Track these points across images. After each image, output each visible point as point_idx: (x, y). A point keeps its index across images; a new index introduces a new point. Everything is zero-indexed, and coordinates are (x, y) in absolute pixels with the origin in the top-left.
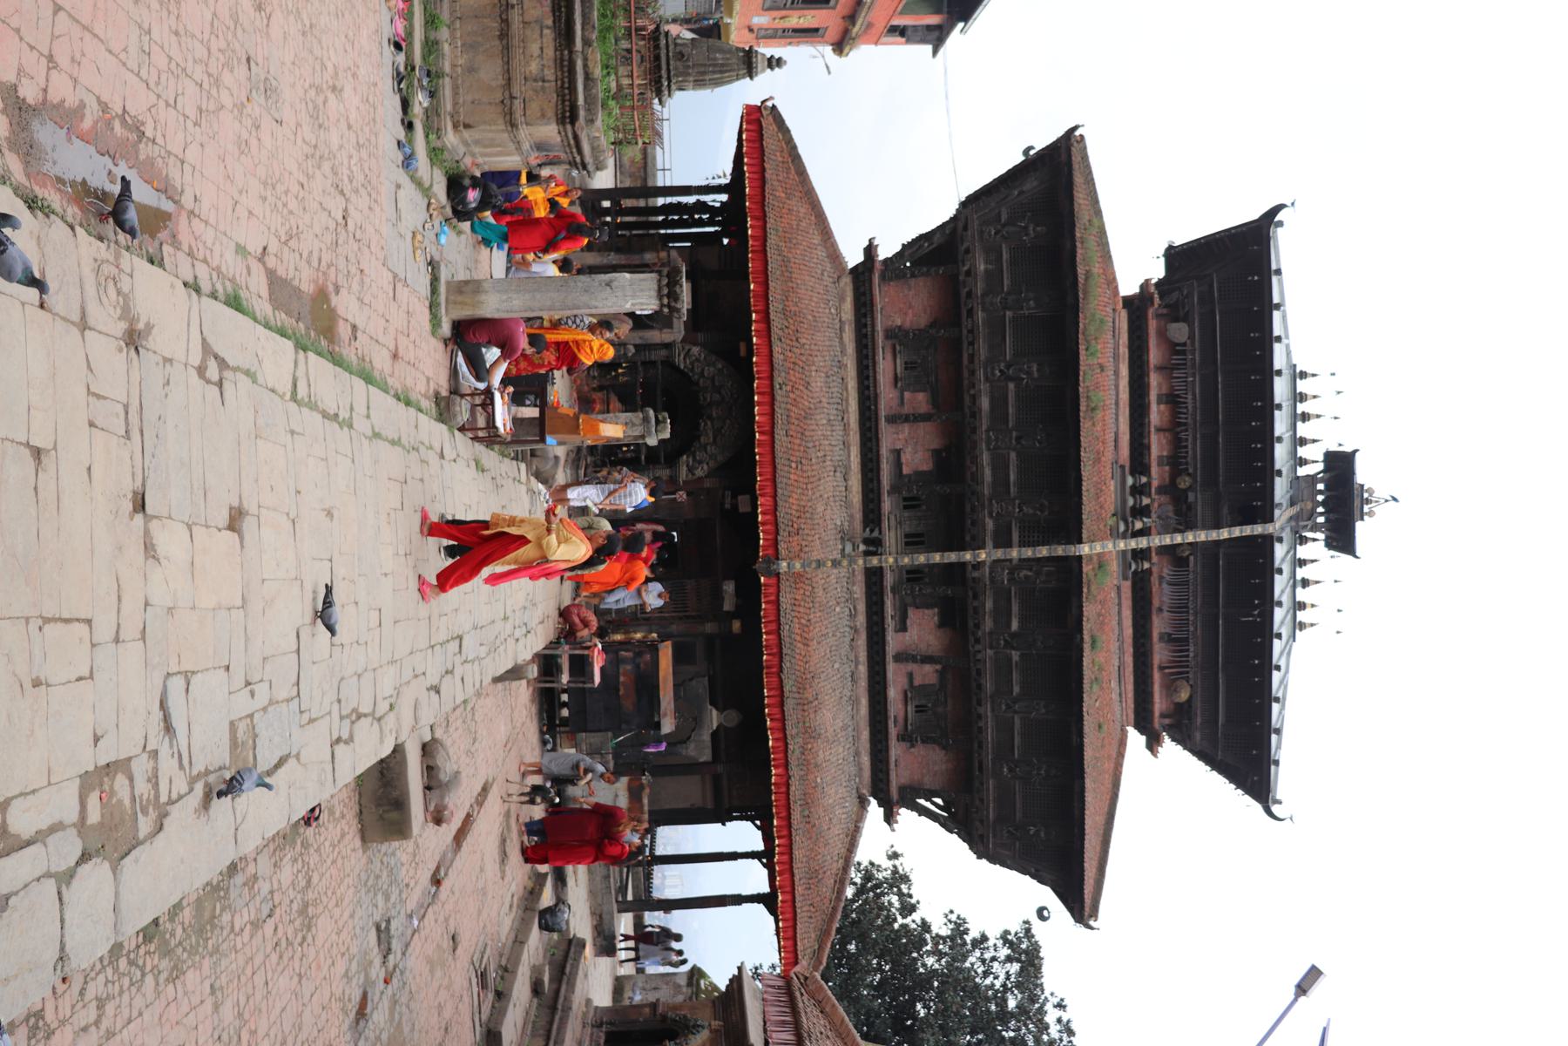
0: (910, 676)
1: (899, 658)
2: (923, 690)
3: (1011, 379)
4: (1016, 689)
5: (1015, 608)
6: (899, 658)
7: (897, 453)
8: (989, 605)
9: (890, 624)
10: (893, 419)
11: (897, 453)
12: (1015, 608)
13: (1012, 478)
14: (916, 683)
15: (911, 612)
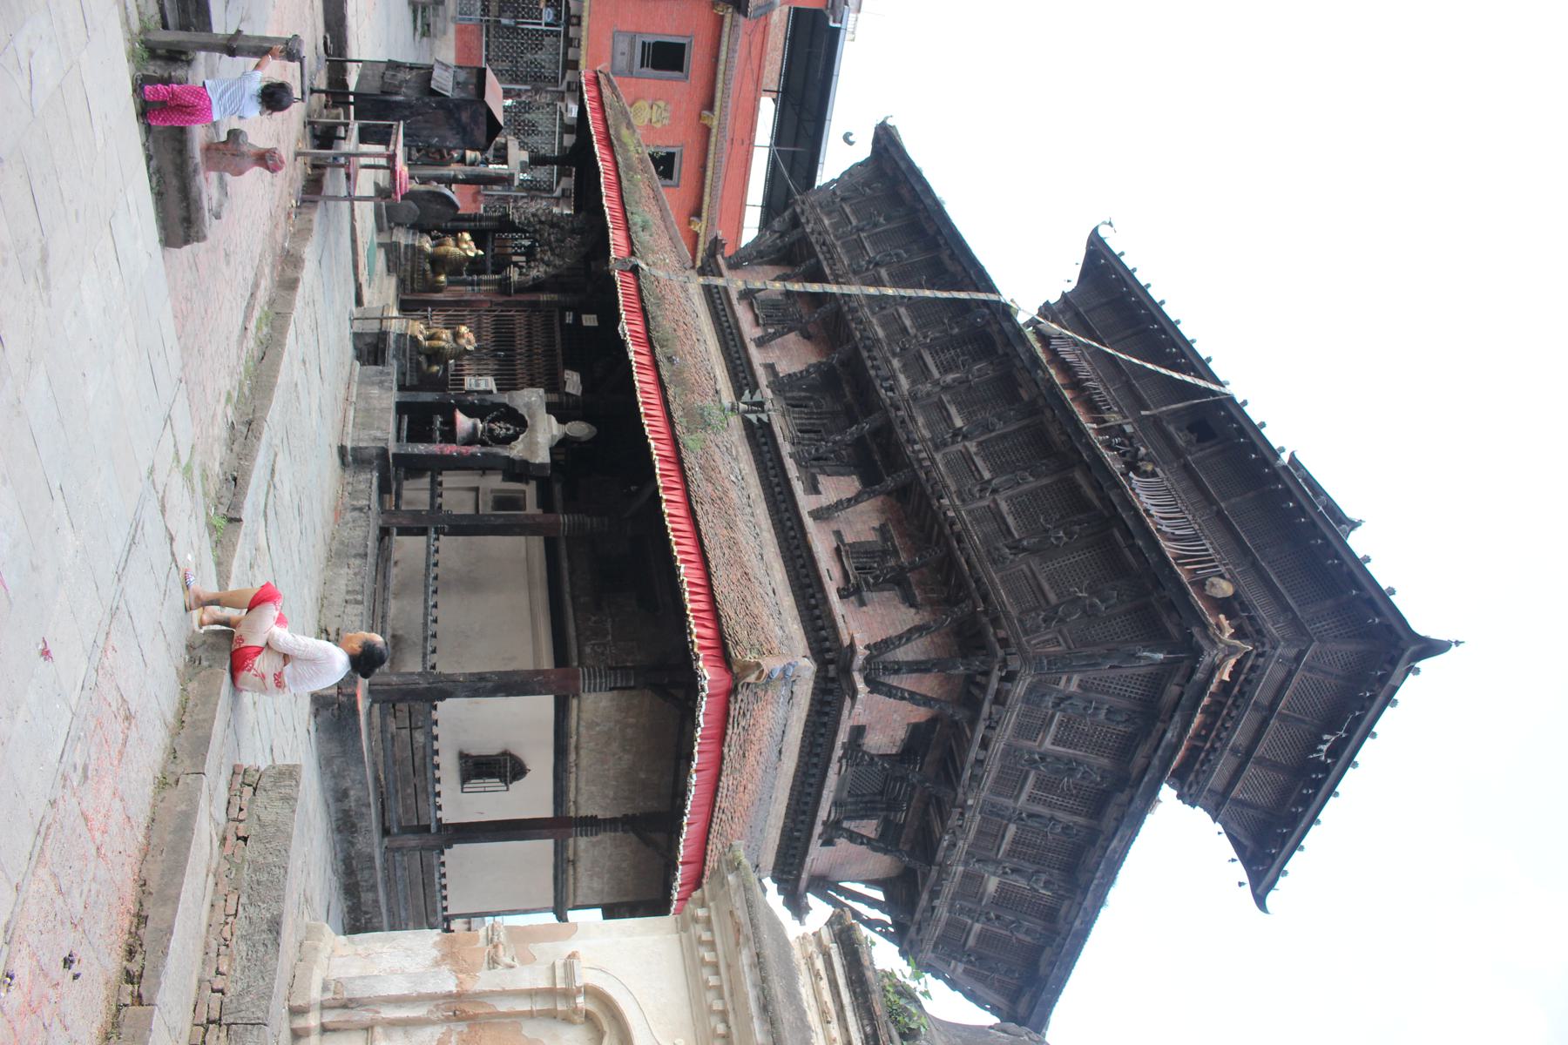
0: (838, 534)
1: (818, 515)
2: (858, 550)
3: (877, 264)
4: (987, 475)
5: (953, 410)
6: (818, 515)
7: (770, 368)
8: (921, 421)
9: (798, 487)
10: (761, 343)
11: (770, 368)
12: (953, 410)
13: (908, 323)
14: (849, 539)
15: (821, 478)
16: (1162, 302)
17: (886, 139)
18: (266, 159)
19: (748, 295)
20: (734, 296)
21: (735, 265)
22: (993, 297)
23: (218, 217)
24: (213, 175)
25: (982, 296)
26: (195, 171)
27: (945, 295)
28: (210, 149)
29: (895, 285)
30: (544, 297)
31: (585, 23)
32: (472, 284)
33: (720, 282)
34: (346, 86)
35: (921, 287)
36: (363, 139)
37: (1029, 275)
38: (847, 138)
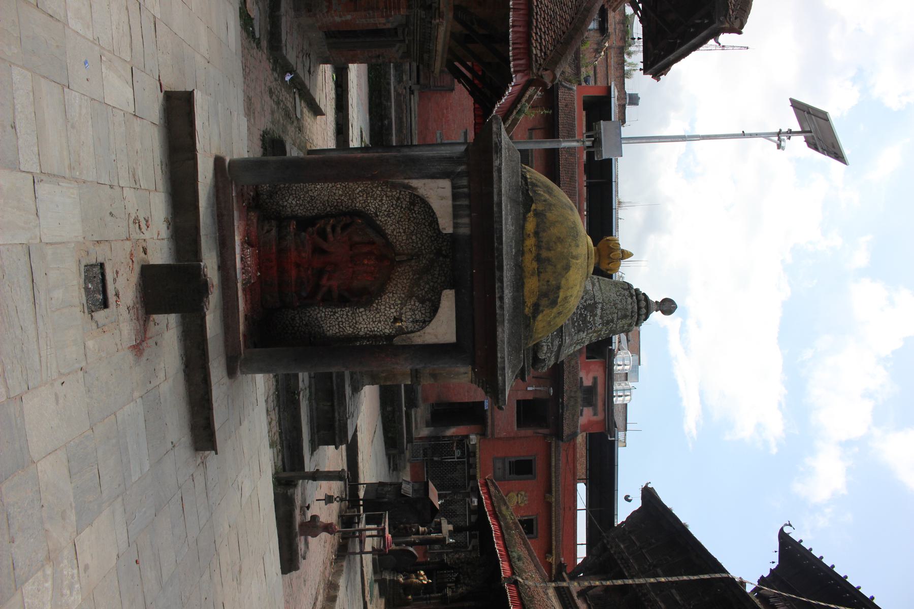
13: (678, 598)
16: (822, 557)
17: (648, 494)
18: (328, 528)
19: (582, 594)
20: (575, 595)
21: (573, 577)
22: (724, 575)
23: (304, 558)
24: (303, 538)
25: (718, 575)
26: (296, 536)
27: (696, 577)
28: (303, 525)
29: (665, 576)
30: (467, 604)
31: (478, 456)
32: (426, 599)
33: (565, 584)
34: (358, 497)
35: (682, 575)
36: (367, 523)
37: (748, 560)
38: (627, 498)
